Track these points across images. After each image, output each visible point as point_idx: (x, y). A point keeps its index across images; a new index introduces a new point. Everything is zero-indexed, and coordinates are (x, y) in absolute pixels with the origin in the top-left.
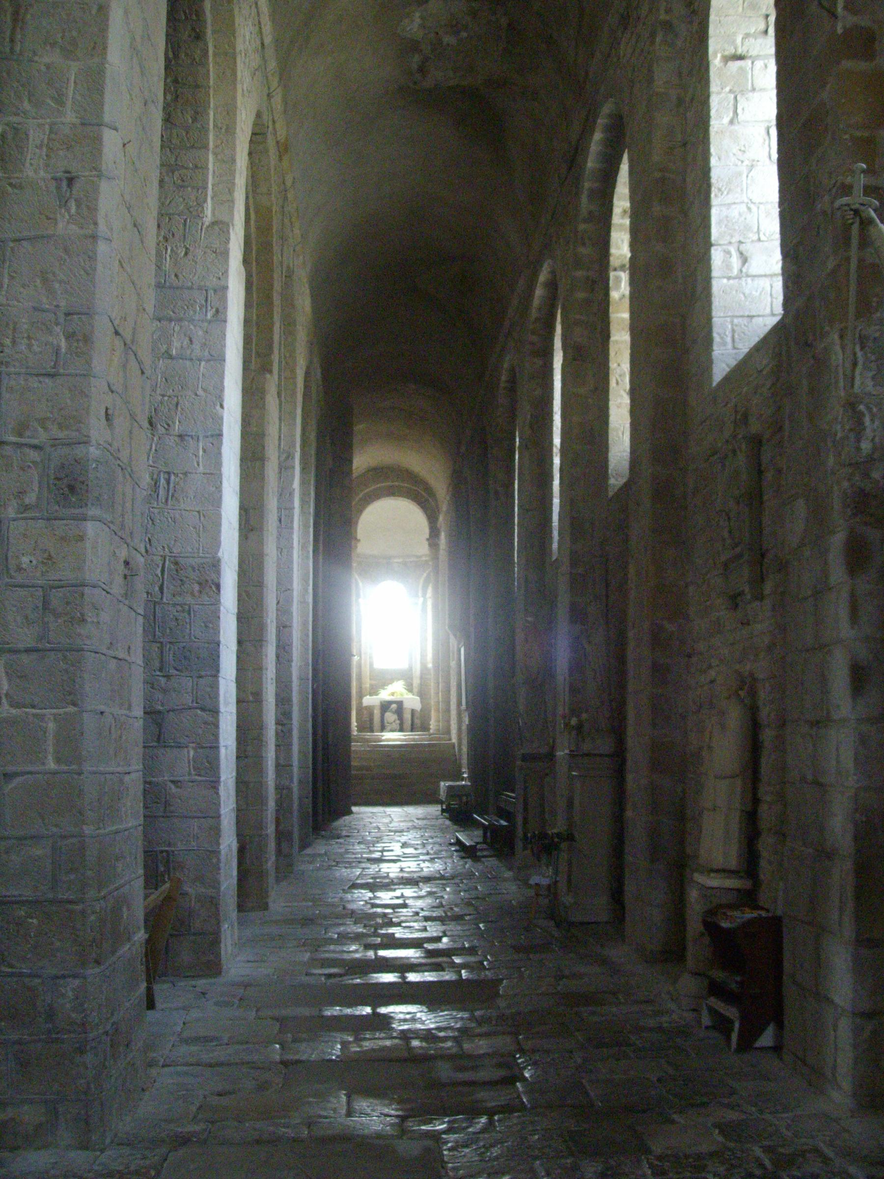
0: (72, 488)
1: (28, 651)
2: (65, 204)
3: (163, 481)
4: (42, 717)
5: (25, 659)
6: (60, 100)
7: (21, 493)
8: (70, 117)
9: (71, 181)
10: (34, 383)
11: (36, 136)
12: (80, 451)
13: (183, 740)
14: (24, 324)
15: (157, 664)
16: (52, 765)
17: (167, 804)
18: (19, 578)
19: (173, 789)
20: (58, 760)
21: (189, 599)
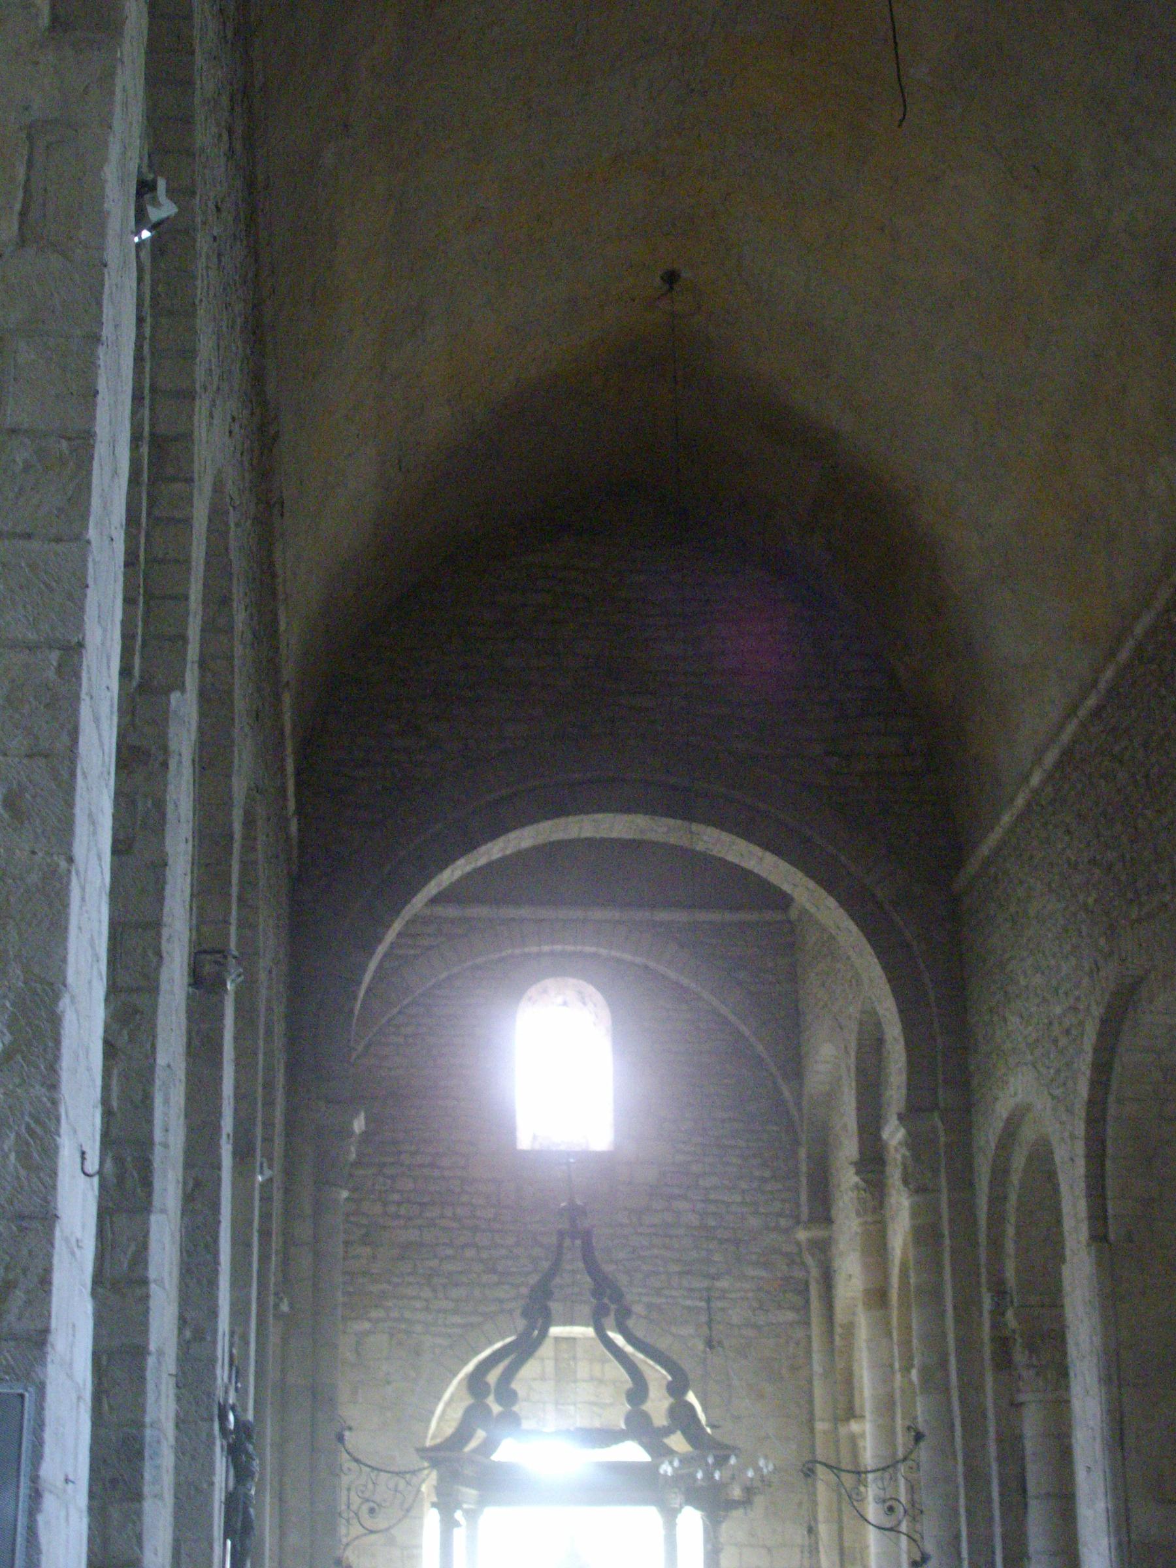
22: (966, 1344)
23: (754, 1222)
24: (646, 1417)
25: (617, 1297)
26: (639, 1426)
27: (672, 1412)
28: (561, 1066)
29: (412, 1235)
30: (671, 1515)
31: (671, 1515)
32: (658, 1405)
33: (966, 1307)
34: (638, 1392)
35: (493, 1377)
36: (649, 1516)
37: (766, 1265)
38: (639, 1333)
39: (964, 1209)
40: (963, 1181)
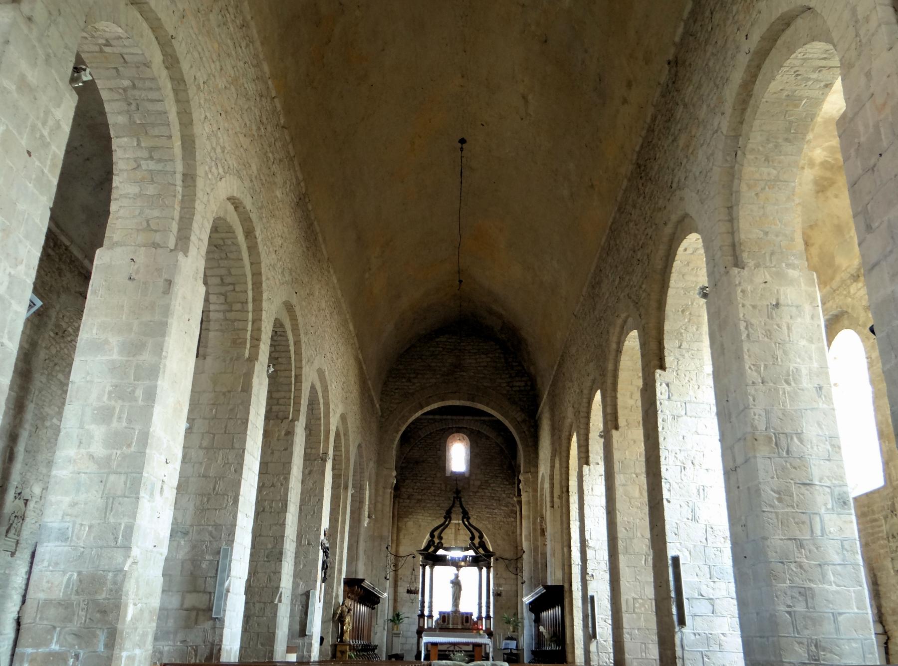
0: (845, 503)
1: (839, 564)
2: (820, 397)
3: (701, 491)
4: (849, 591)
5: (838, 568)
6: (810, 358)
7: (825, 504)
8: (815, 365)
9: (820, 388)
10: (822, 462)
11: (804, 371)
12: (845, 489)
13: (725, 613)
14: (814, 441)
15: (709, 576)
16: (856, 611)
17: (720, 645)
18: (831, 537)
19: (722, 637)
20: (858, 608)
21: (719, 545)
22: (535, 530)
23: (504, 495)
24: (474, 545)
25: (467, 513)
26: (472, 547)
27: (479, 543)
28: (458, 456)
29: (420, 497)
30: (480, 569)
31: (480, 569)
32: (477, 541)
33: (534, 523)
34: (472, 538)
35: (436, 534)
36: (475, 569)
37: (507, 506)
38: (474, 524)
39: (535, 497)
40: (535, 490)
